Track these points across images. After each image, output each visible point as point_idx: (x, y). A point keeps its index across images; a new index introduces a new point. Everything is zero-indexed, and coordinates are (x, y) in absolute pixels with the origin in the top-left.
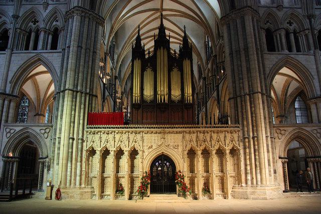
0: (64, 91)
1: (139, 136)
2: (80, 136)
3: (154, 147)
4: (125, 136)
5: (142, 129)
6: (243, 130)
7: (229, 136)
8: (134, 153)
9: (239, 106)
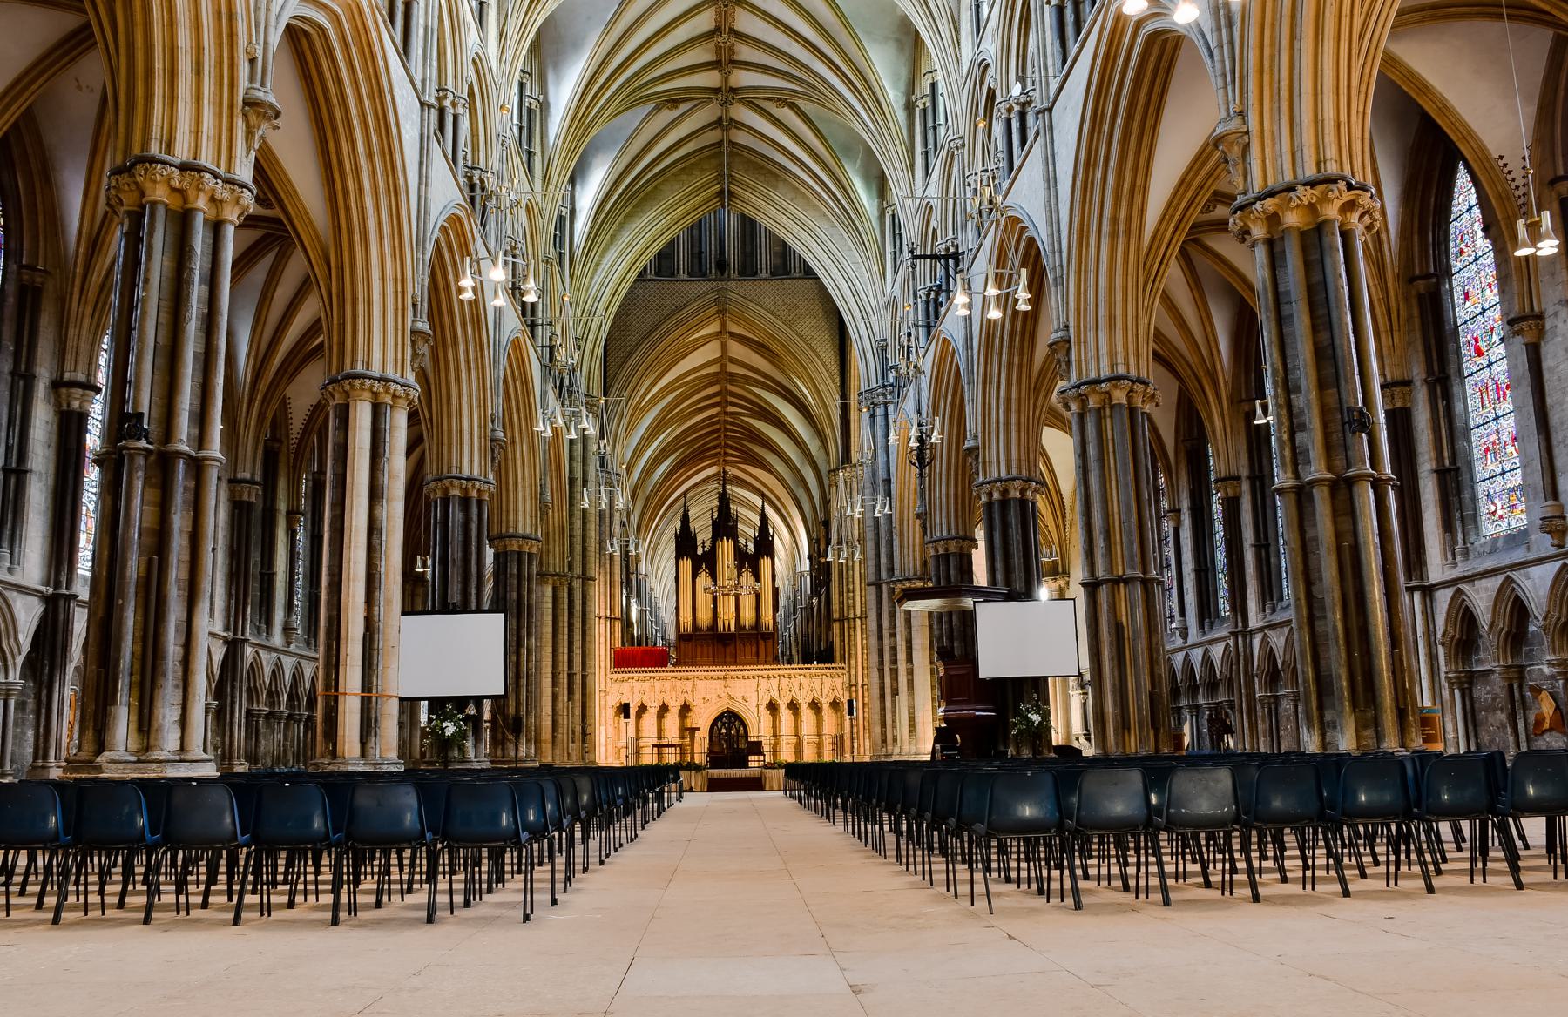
1: (689, 684)
2: (603, 688)
3: (714, 701)
4: (668, 684)
5: (696, 674)
6: (849, 672)
7: (828, 681)
8: (685, 709)
9: (846, 634)
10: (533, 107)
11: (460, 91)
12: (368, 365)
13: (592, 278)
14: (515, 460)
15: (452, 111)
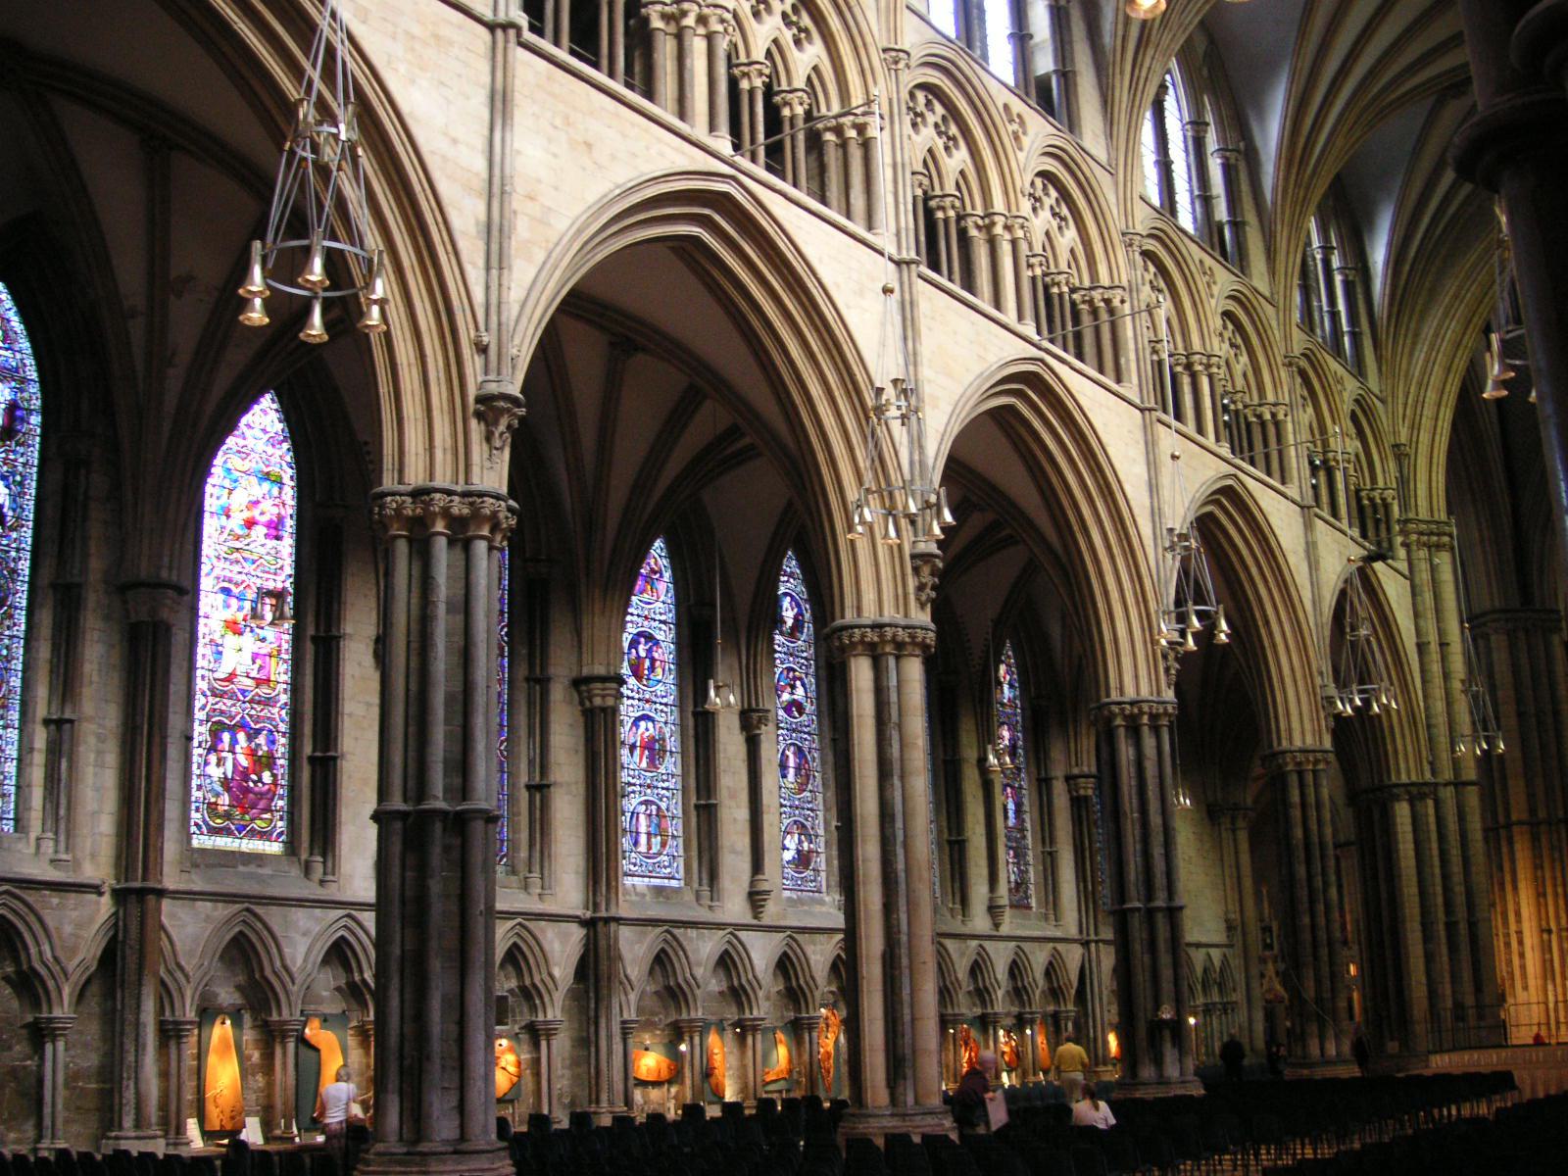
0: (1509, 826)
10: (1232, 161)
11: (1014, 208)
12: (859, 614)
13: (1411, 354)
14: (1274, 646)
15: (1007, 236)
